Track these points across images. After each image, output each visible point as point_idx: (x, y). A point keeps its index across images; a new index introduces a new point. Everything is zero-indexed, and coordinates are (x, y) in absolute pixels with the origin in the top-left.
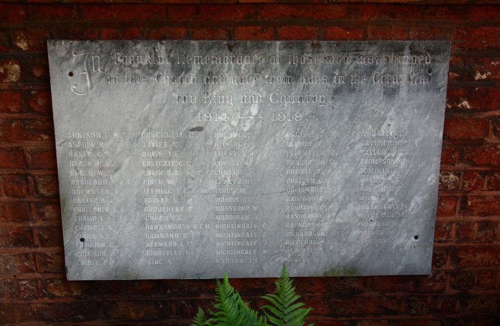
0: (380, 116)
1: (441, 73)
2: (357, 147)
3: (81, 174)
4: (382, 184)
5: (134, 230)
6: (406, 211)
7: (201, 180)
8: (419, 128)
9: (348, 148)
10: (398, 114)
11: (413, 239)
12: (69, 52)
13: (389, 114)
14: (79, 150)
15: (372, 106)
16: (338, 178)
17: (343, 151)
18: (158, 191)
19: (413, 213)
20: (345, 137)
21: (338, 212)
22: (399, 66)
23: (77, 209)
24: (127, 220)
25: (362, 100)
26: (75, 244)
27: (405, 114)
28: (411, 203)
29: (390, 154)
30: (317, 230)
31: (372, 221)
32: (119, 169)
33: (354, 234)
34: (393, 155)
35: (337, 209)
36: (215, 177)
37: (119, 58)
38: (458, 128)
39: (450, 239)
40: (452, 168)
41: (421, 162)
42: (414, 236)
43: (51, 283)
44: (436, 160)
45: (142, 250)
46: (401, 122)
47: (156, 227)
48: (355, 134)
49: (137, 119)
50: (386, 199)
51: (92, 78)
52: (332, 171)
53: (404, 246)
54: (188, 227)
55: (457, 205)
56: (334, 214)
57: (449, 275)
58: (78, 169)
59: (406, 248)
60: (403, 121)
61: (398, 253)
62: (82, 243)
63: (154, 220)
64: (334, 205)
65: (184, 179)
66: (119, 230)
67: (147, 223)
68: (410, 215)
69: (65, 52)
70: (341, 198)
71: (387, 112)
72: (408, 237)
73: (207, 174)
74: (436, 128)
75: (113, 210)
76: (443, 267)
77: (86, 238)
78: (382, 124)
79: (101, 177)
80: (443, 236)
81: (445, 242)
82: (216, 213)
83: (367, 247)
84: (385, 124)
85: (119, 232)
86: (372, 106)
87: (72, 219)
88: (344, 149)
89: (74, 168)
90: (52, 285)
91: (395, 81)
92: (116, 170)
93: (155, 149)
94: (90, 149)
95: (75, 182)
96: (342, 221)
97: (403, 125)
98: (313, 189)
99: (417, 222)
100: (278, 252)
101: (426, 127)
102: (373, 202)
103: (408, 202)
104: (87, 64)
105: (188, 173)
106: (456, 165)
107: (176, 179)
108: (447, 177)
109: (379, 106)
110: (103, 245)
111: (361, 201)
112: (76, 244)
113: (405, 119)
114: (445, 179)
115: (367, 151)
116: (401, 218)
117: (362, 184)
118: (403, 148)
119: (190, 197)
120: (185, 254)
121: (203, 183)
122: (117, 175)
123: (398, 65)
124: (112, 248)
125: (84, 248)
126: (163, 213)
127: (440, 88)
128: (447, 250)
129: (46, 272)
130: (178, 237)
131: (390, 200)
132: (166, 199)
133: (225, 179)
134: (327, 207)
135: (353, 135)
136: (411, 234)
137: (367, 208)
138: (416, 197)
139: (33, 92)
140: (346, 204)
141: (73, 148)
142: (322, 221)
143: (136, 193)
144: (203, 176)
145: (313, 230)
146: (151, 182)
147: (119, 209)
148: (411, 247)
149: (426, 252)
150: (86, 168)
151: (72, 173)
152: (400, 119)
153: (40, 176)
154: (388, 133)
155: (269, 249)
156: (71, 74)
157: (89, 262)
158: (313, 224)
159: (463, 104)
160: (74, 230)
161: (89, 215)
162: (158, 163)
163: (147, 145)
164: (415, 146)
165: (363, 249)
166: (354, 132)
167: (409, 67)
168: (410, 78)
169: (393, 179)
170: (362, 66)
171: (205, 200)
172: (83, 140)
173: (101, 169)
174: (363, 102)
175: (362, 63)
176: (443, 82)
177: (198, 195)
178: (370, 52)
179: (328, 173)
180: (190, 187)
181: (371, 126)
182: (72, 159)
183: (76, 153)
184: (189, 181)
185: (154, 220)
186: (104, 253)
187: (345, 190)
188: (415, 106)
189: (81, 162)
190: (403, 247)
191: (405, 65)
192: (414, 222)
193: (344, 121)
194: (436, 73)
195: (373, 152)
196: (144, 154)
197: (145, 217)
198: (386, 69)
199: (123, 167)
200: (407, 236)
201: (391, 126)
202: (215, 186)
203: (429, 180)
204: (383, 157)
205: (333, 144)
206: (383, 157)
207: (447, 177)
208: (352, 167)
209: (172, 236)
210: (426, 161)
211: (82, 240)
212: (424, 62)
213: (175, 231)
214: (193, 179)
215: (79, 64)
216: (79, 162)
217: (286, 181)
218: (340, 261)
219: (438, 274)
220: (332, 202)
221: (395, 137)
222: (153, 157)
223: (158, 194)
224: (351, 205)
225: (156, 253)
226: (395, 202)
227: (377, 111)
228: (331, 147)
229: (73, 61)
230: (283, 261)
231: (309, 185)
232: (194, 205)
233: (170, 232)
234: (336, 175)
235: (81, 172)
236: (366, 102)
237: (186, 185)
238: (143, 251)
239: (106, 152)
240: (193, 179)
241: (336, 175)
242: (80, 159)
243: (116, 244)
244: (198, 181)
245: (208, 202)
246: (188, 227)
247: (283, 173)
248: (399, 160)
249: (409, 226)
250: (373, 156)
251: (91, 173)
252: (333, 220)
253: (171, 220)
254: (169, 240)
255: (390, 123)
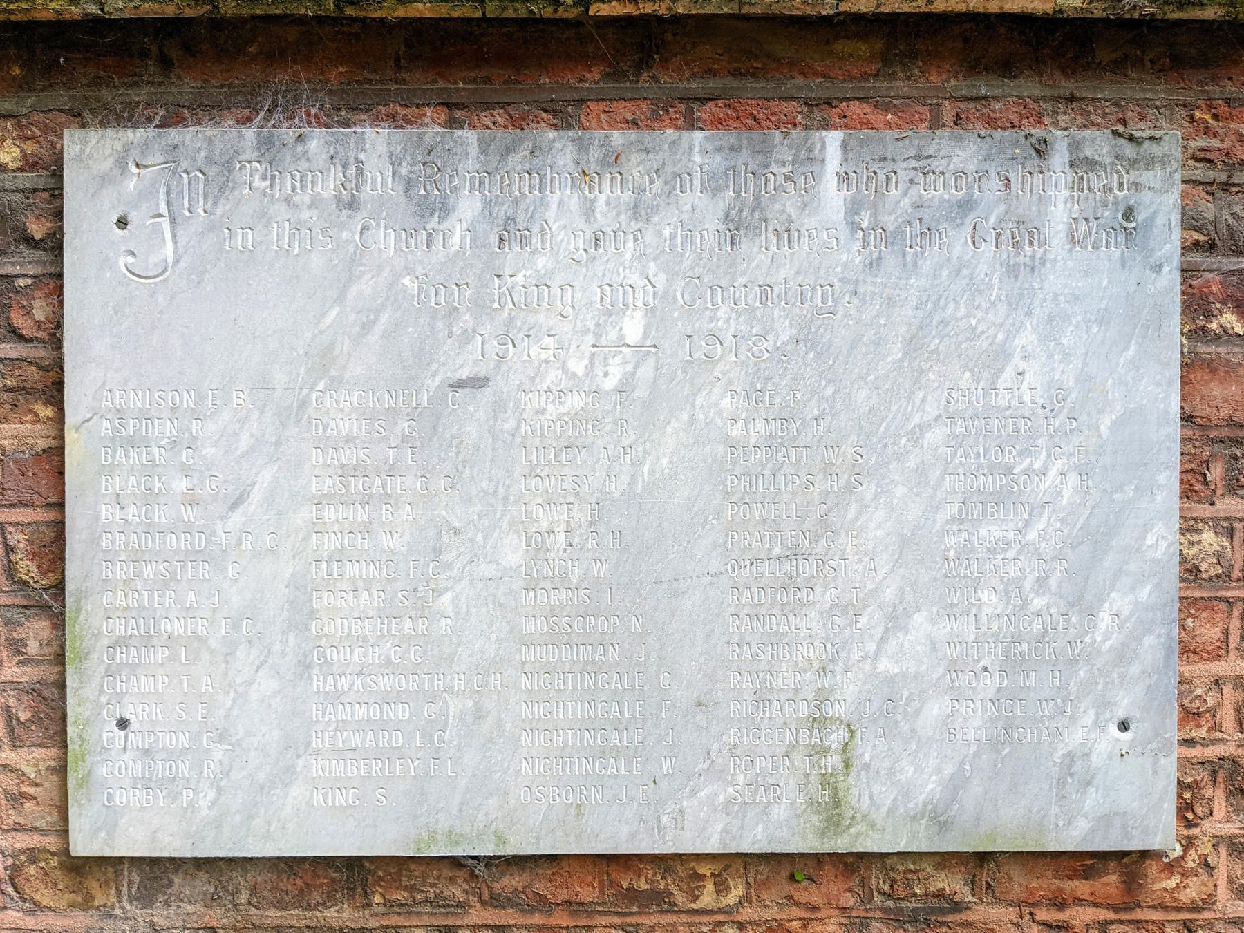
0: (994, 347)
1: (1160, 221)
2: (931, 437)
3: (130, 518)
4: (1010, 554)
5: (279, 692)
6: (1087, 639)
7: (480, 537)
8: (1110, 382)
9: (904, 441)
10: (1043, 339)
11: (1113, 730)
12: (121, 164)
13: (1019, 342)
14: (131, 442)
15: (969, 315)
16: (880, 533)
17: (889, 451)
18: (351, 570)
19: (1108, 644)
20: (894, 408)
21: (883, 640)
22: (1040, 200)
23: (114, 623)
24: (257, 663)
25: (939, 300)
26: (100, 736)
27: (1064, 341)
28: (1101, 614)
29: (1028, 460)
30: (822, 697)
31: (985, 669)
32: (242, 503)
33: (935, 711)
34: (1037, 465)
35: (879, 632)
36: (521, 527)
37: (257, 177)
38: (1217, 392)
39: (1218, 735)
40: (1208, 511)
41: (1121, 488)
42: (1116, 721)
43: (33, 863)
44: (1169, 480)
45: (298, 756)
46: (1056, 365)
47: (343, 684)
48: (924, 400)
49: (301, 352)
50: (1025, 602)
51: (180, 232)
52: (859, 513)
53: (1088, 755)
54: (439, 685)
55: (1231, 627)
56: (871, 647)
57: (1223, 851)
58: (124, 502)
59: (1094, 758)
60: (1061, 361)
61: (1071, 775)
62: (122, 733)
63: (339, 661)
64: (871, 617)
65: (432, 533)
66: (232, 694)
67: (316, 670)
68: (1099, 652)
69: (111, 161)
70: (889, 594)
71: (1010, 336)
72: (1100, 726)
73: (498, 516)
74: (1159, 384)
75: (220, 627)
76: (1206, 825)
77: (133, 719)
78: (1001, 371)
79: (188, 527)
80: (1198, 726)
81: (1206, 743)
82: (525, 642)
83: (977, 754)
84: (1009, 372)
85: (234, 701)
86: (969, 315)
87: (95, 656)
88: (894, 444)
89: (114, 499)
90: (32, 870)
91: (1031, 243)
92: (234, 506)
93: (349, 440)
94: (163, 439)
95: (113, 542)
96: (896, 671)
97: (1063, 372)
98: (806, 568)
99: (1122, 677)
100: (705, 766)
101: (1129, 378)
102: (987, 610)
103: (1092, 614)
104: (168, 194)
105: (444, 513)
106: (1219, 505)
107: (407, 533)
108: (1195, 538)
109: (990, 317)
110: (184, 741)
111: (952, 605)
112: (105, 736)
113: (1066, 356)
114: (1191, 543)
115: (960, 452)
116: (1074, 661)
117: (952, 554)
118: (1067, 444)
119: (447, 589)
120: (427, 773)
121: (484, 547)
122: (236, 518)
123: (1035, 198)
124: (208, 751)
125: (125, 749)
126: (365, 639)
127: (1161, 266)
128: (1214, 768)
129: (18, 828)
130: (407, 715)
131: (1038, 603)
132: (376, 594)
133: (551, 532)
134: (850, 625)
135: (918, 401)
136: (1108, 716)
137: (968, 629)
138: (1113, 594)
139: (21, 282)
140: (908, 615)
141: (113, 439)
142: (838, 669)
143: (288, 574)
144: (485, 523)
145: (810, 698)
146: (332, 543)
147: (235, 625)
148: (1110, 758)
149: (1155, 772)
150: (149, 499)
151: (106, 513)
152: (1051, 356)
153: (22, 526)
154: (1020, 398)
155: (680, 758)
156: (122, 223)
157: (138, 797)
158: (808, 676)
159: (1222, 320)
160: (101, 691)
161: (147, 641)
162: (357, 485)
163: (325, 428)
164: (1100, 436)
165: (962, 763)
166: (921, 394)
167: (1069, 205)
168: (1073, 237)
169: (1042, 535)
170: (936, 200)
171: (490, 598)
172: (145, 415)
173: (191, 501)
174: (942, 303)
175: (941, 193)
176: (1168, 246)
177: (471, 581)
178: (955, 159)
179: (848, 519)
180: (448, 556)
181: (968, 374)
182: (109, 470)
183: (120, 451)
184: (446, 539)
185: (339, 661)
186: (184, 768)
187: (902, 571)
188: (1093, 318)
189: (133, 480)
190: (1086, 755)
191: (1057, 199)
192: (1115, 675)
193: (890, 359)
194: (1146, 220)
195: (978, 454)
196: (316, 457)
197: (311, 651)
198: (1002, 208)
199: (256, 495)
200: (1096, 722)
201: (1027, 376)
202: (521, 554)
203: (1149, 542)
204: (1008, 470)
205: (861, 428)
206: (1008, 470)
207: (1195, 538)
208: (918, 499)
209: (389, 712)
210: (1136, 482)
211: (123, 724)
212: (1111, 190)
213: (396, 698)
214: (457, 532)
215: (146, 194)
216: (127, 481)
217: (725, 542)
218: (895, 799)
219: (1193, 851)
220: (865, 607)
221: (1040, 411)
222: (343, 466)
223: (353, 579)
224: (919, 618)
225: (337, 768)
226: (1053, 611)
227: (983, 332)
228: (854, 437)
229: (132, 184)
230: (722, 798)
231: (793, 555)
232: (458, 613)
233: (387, 699)
234: (872, 525)
235: (132, 509)
236: (951, 306)
237: (437, 551)
238: (301, 762)
239: (209, 451)
240: (457, 532)
241: (872, 525)
242: (131, 472)
243: (222, 738)
244: (471, 540)
245: (500, 605)
246: (439, 685)
247: (718, 516)
248: (1056, 478)
249: (1100, 687)
250: (980, 466)
251: (161, 515)
252: (867, 666)
253: (389, 662)
254: (383, 725)
255: (1022, 366)
